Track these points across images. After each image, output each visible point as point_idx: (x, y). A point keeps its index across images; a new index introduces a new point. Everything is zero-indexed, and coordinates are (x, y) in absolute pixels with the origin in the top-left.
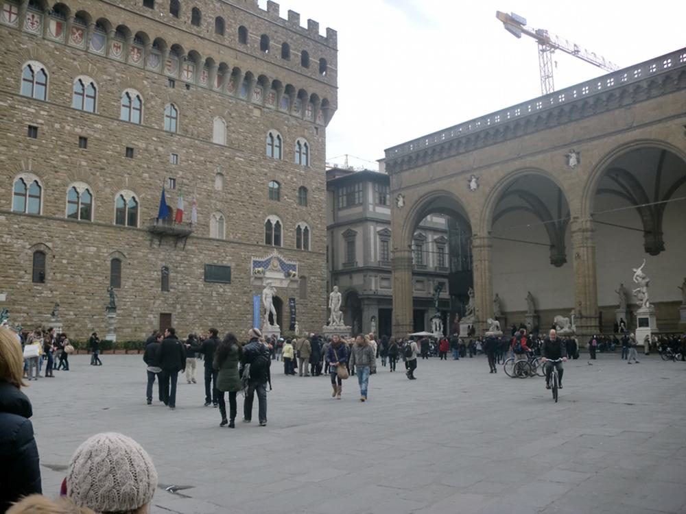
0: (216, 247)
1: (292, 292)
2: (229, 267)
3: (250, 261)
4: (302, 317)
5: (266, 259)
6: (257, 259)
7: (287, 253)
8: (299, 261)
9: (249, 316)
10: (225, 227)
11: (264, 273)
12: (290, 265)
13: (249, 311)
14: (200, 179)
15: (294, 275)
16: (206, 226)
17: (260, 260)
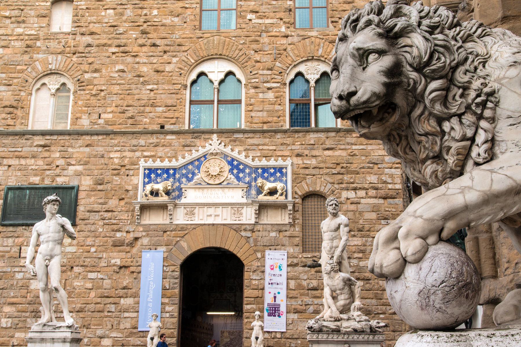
0: (40, 149)
1: (273, 234)
2: (72, 188)
3: (138, 169)
4: (307, 300)
5: (182, 161)
6: (158, 164)
7: (255, 141)
8: (298, 155)
9: (129, 301)
10: (71, 103)
11: (175, 194)
12: (265, 170)
13: (124, 288)
14: (10, 18)
15: (273, 192)
16: (17, 107)
17: (166, 164)
